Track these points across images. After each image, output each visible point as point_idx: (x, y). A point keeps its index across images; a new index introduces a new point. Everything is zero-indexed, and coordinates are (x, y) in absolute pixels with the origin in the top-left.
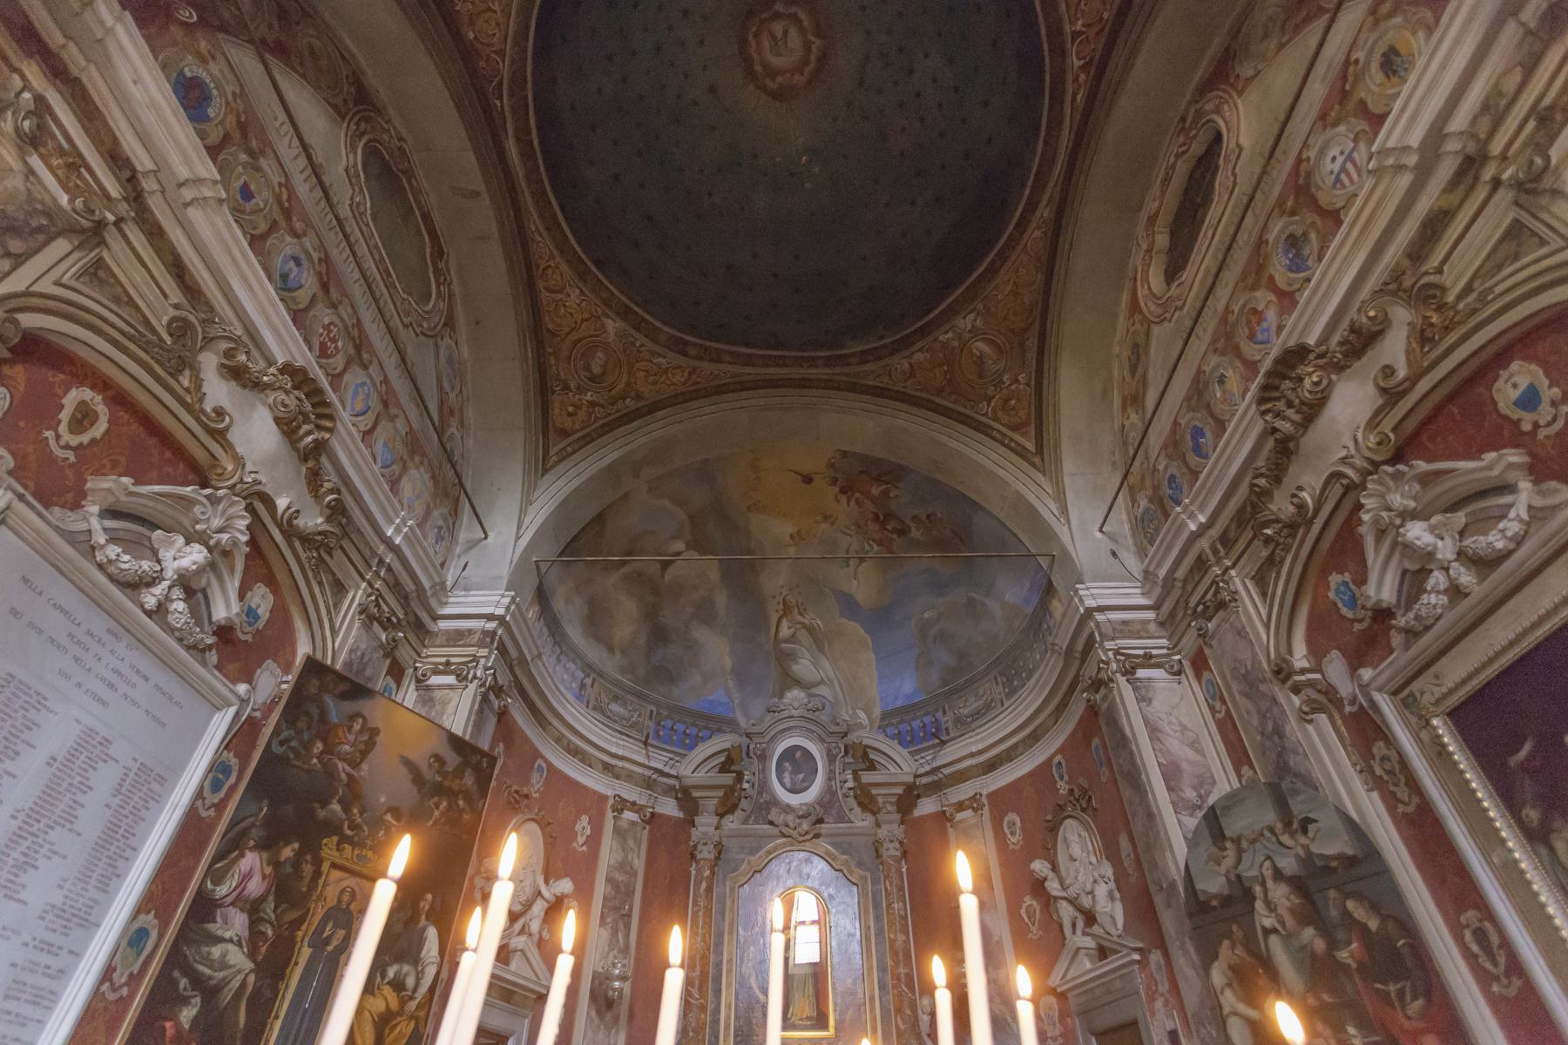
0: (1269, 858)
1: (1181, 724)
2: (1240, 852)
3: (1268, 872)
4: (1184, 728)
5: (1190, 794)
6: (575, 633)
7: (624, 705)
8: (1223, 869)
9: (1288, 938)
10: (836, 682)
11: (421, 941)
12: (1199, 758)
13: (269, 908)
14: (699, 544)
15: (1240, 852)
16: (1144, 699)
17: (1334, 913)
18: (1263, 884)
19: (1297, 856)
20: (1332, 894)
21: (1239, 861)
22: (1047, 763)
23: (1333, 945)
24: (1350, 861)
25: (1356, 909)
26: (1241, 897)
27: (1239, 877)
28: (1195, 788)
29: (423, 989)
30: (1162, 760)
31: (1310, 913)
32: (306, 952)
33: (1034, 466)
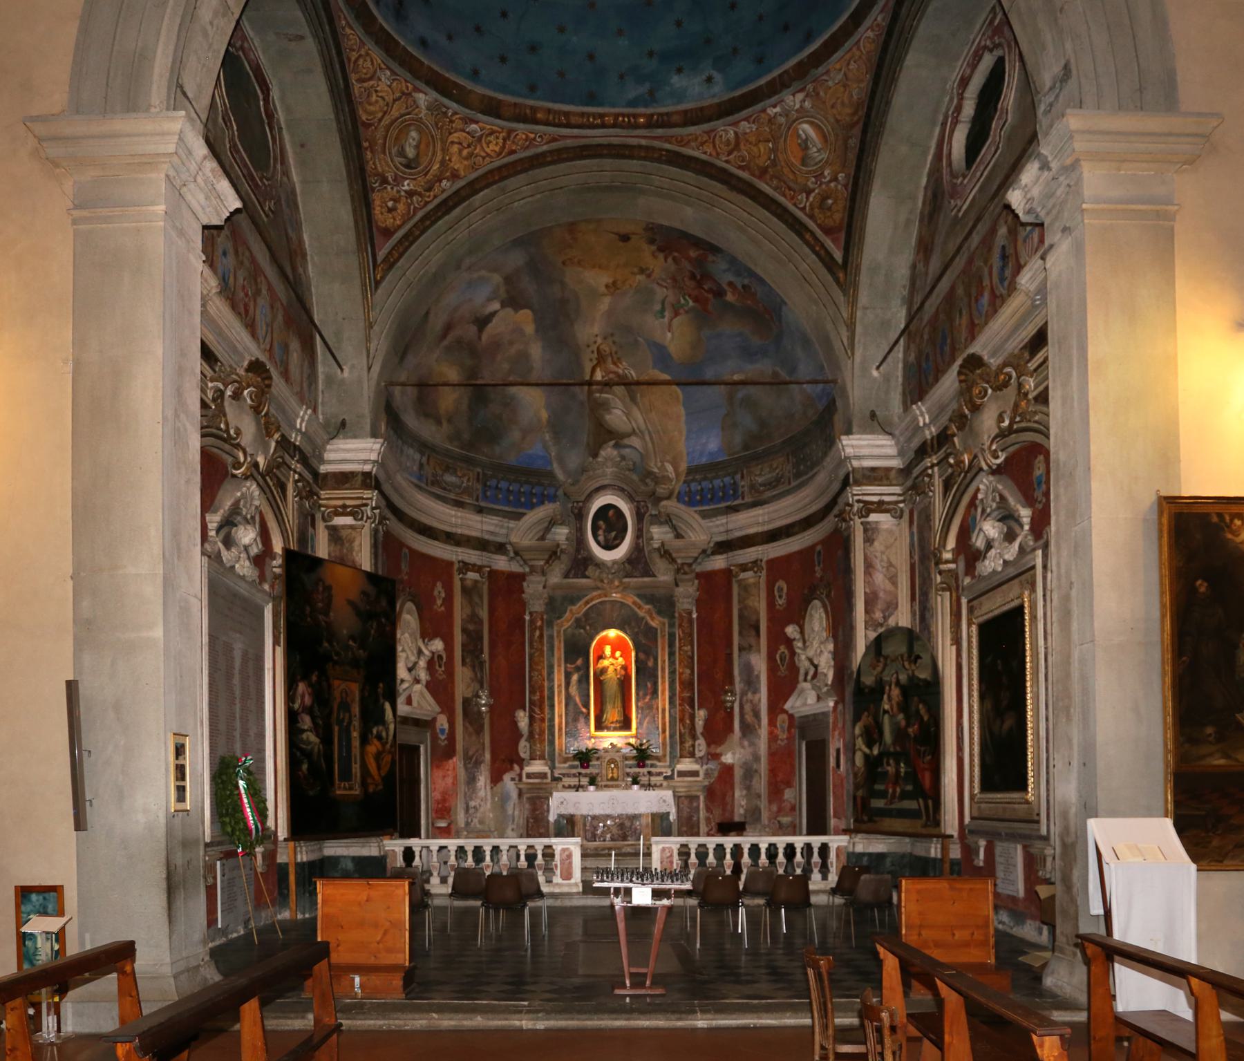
0: (897, 673)
1: (888, 559)
2: (885, 665)
3: (894, 680)
4: (890, 565)
5: (878, 615)
6: (411, 420)
7: (454, 473)
8: (875, 673)
9: (892, 717)
10: (647, 438)
11: (383, 711)
12: (892, 589)
13: (316, 708)
14: (513, 301)
15: (885, 665)
16: (869, 540)
17: (913, 708)
18: (890, 686)
19: (908, 675)
20: (916, 699)
21: (884, 669)
22: (811, 548)
23: (908, 725)
24: (927, 683)
25: (922, 709)
26: (879, 689)
27: (881, 679)
28: (883, 612)
29: (391, 738)
30: (867, 590)
31: (904, 707)
32: (336, 728)
33: (837, 281)
